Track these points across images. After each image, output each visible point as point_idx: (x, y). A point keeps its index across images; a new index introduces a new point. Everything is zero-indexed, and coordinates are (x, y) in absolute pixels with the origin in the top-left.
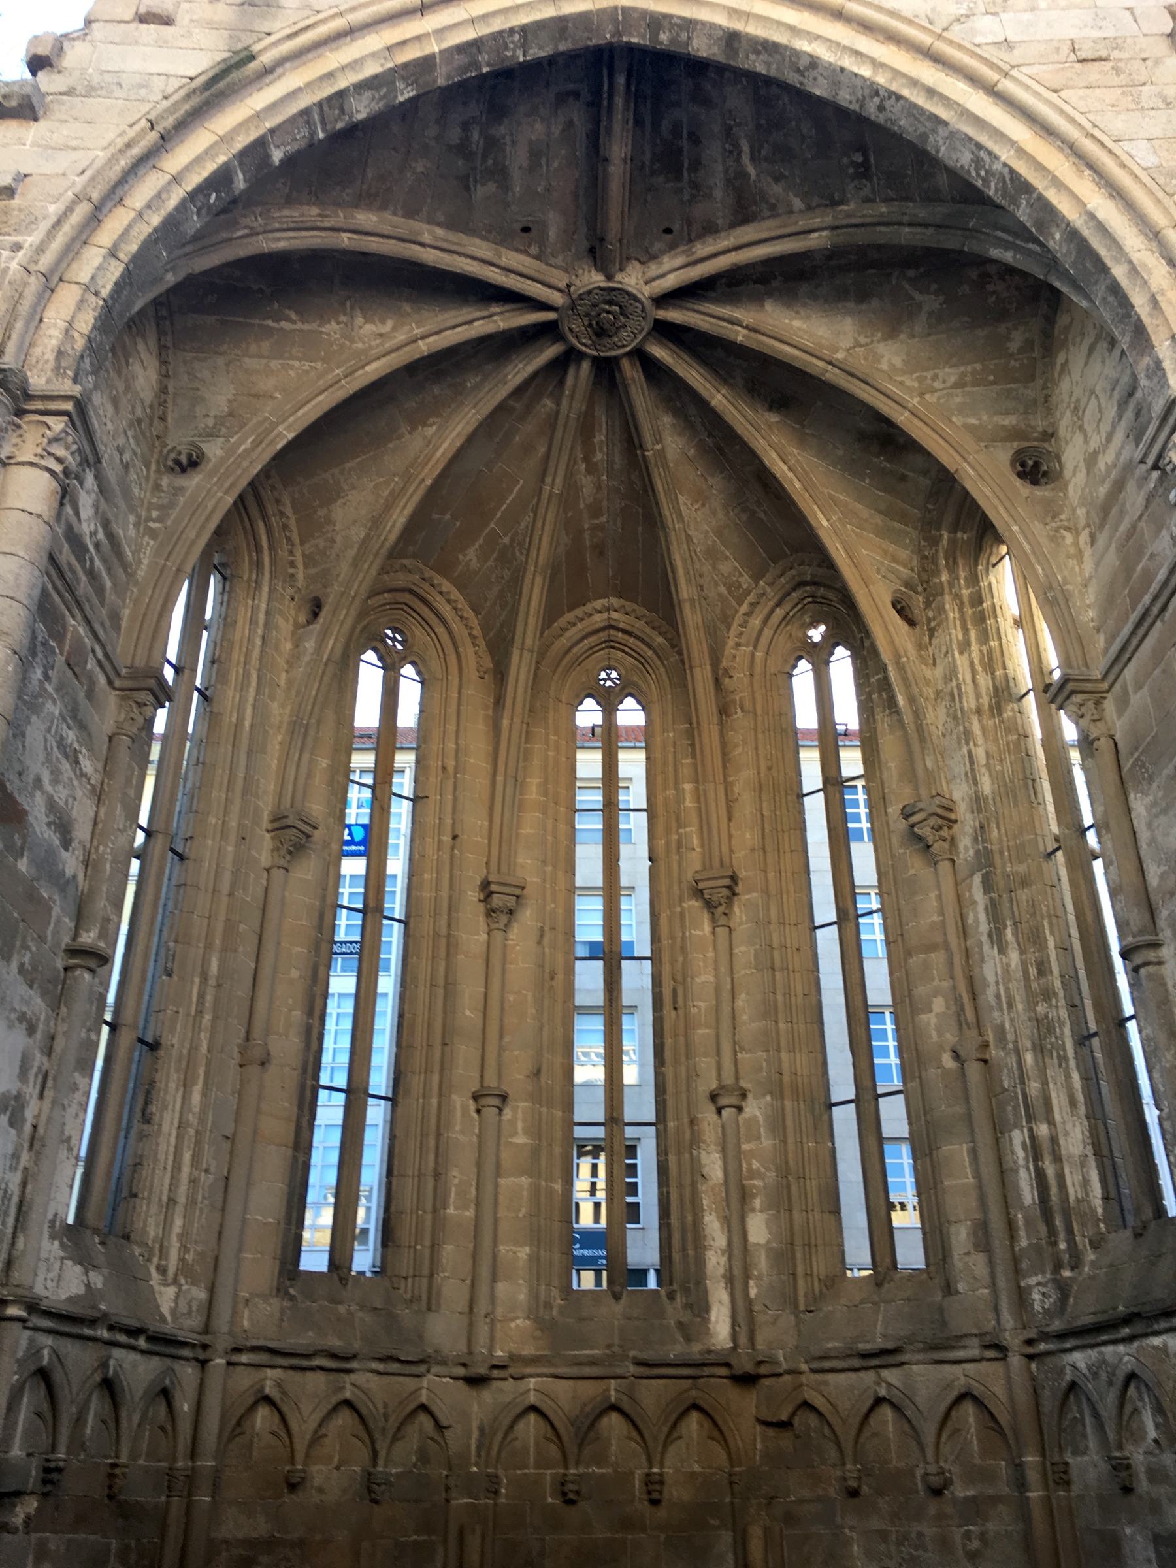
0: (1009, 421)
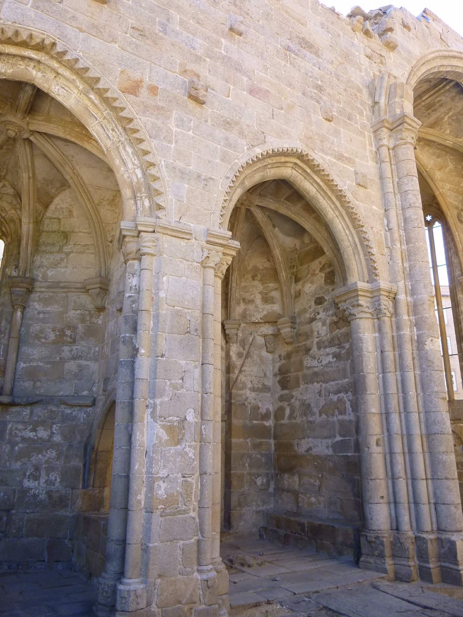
0: (456, 203)
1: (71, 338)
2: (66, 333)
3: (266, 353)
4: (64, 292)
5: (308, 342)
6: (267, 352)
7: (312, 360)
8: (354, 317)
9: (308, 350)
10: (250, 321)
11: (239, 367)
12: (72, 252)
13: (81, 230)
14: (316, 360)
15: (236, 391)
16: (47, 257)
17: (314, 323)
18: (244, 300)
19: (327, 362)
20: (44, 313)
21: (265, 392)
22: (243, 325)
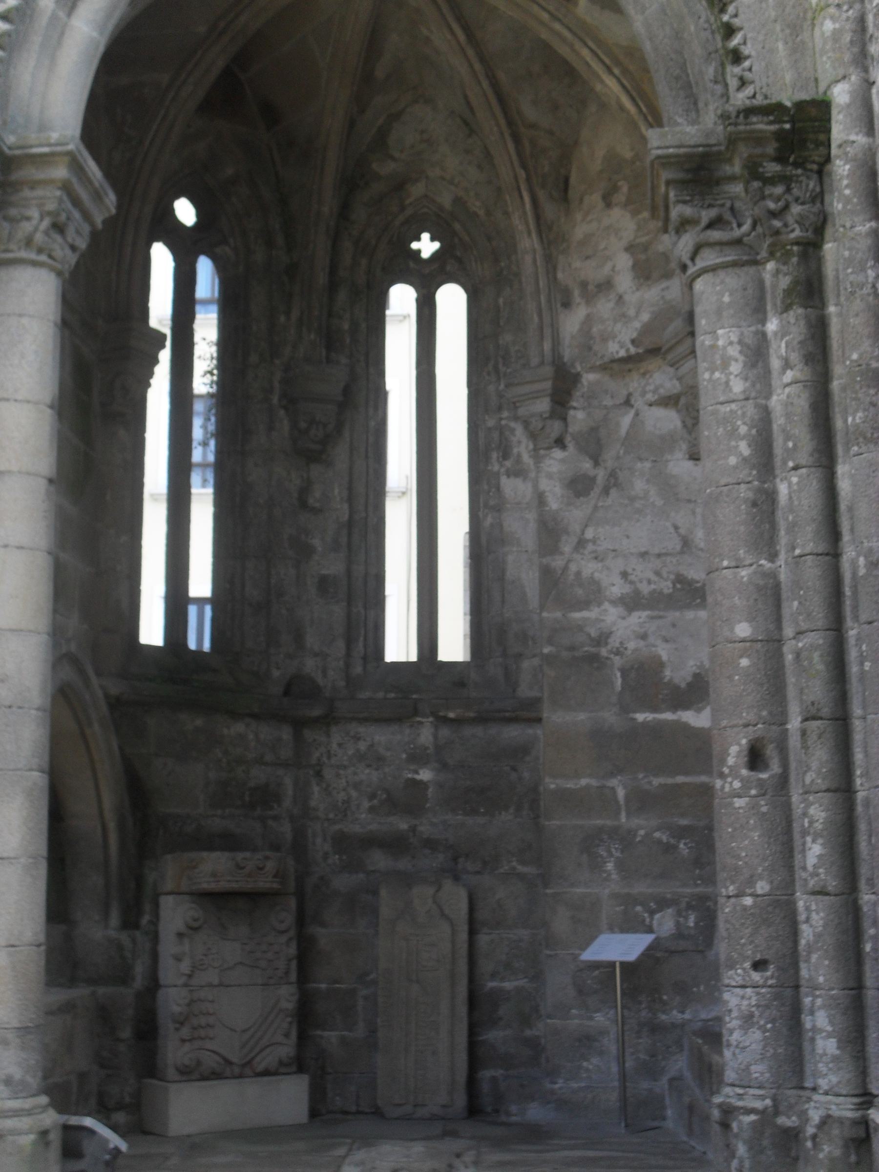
10: (602, 357)
11: (576, 528)
15: (558, 614)
18: (584, 285)
21: (688, 606)
22: (589, 378)
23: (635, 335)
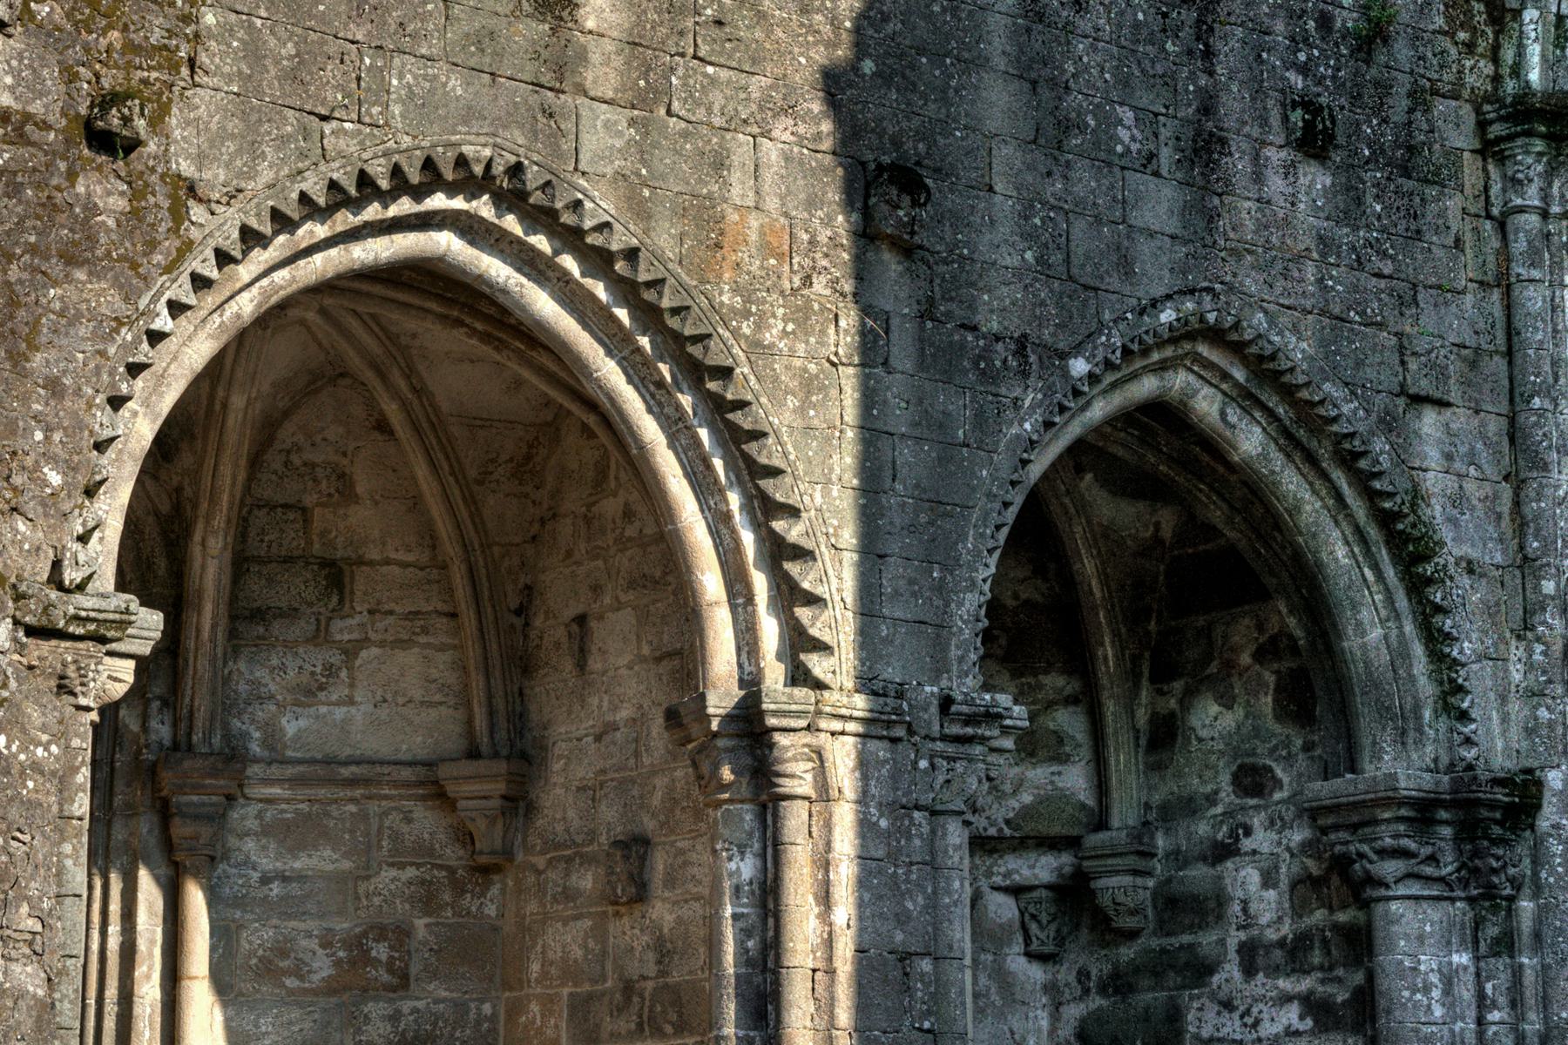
1: (391, 970)
2: (374, 953)
3: (1023, 960)
4: (352, 800)
5: (1207, 940)
6: (1029, 955)
7: (1219, 1013)
8: (1383, 892)
9: (1201, 970)
12: (364, 642)
13: (393, 555)
14: (1236, 1015)
16: (275, 662)
17: (1229, 864)
19: (1277, 1028)
20: (285, 879)
23: (1011, 815)
